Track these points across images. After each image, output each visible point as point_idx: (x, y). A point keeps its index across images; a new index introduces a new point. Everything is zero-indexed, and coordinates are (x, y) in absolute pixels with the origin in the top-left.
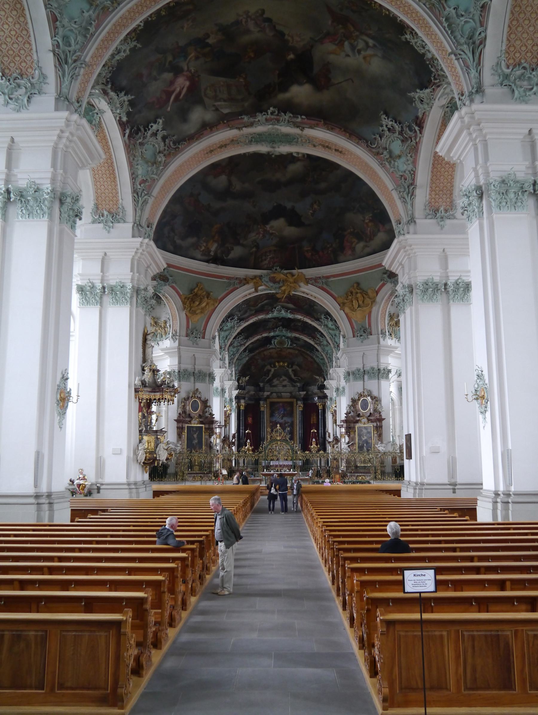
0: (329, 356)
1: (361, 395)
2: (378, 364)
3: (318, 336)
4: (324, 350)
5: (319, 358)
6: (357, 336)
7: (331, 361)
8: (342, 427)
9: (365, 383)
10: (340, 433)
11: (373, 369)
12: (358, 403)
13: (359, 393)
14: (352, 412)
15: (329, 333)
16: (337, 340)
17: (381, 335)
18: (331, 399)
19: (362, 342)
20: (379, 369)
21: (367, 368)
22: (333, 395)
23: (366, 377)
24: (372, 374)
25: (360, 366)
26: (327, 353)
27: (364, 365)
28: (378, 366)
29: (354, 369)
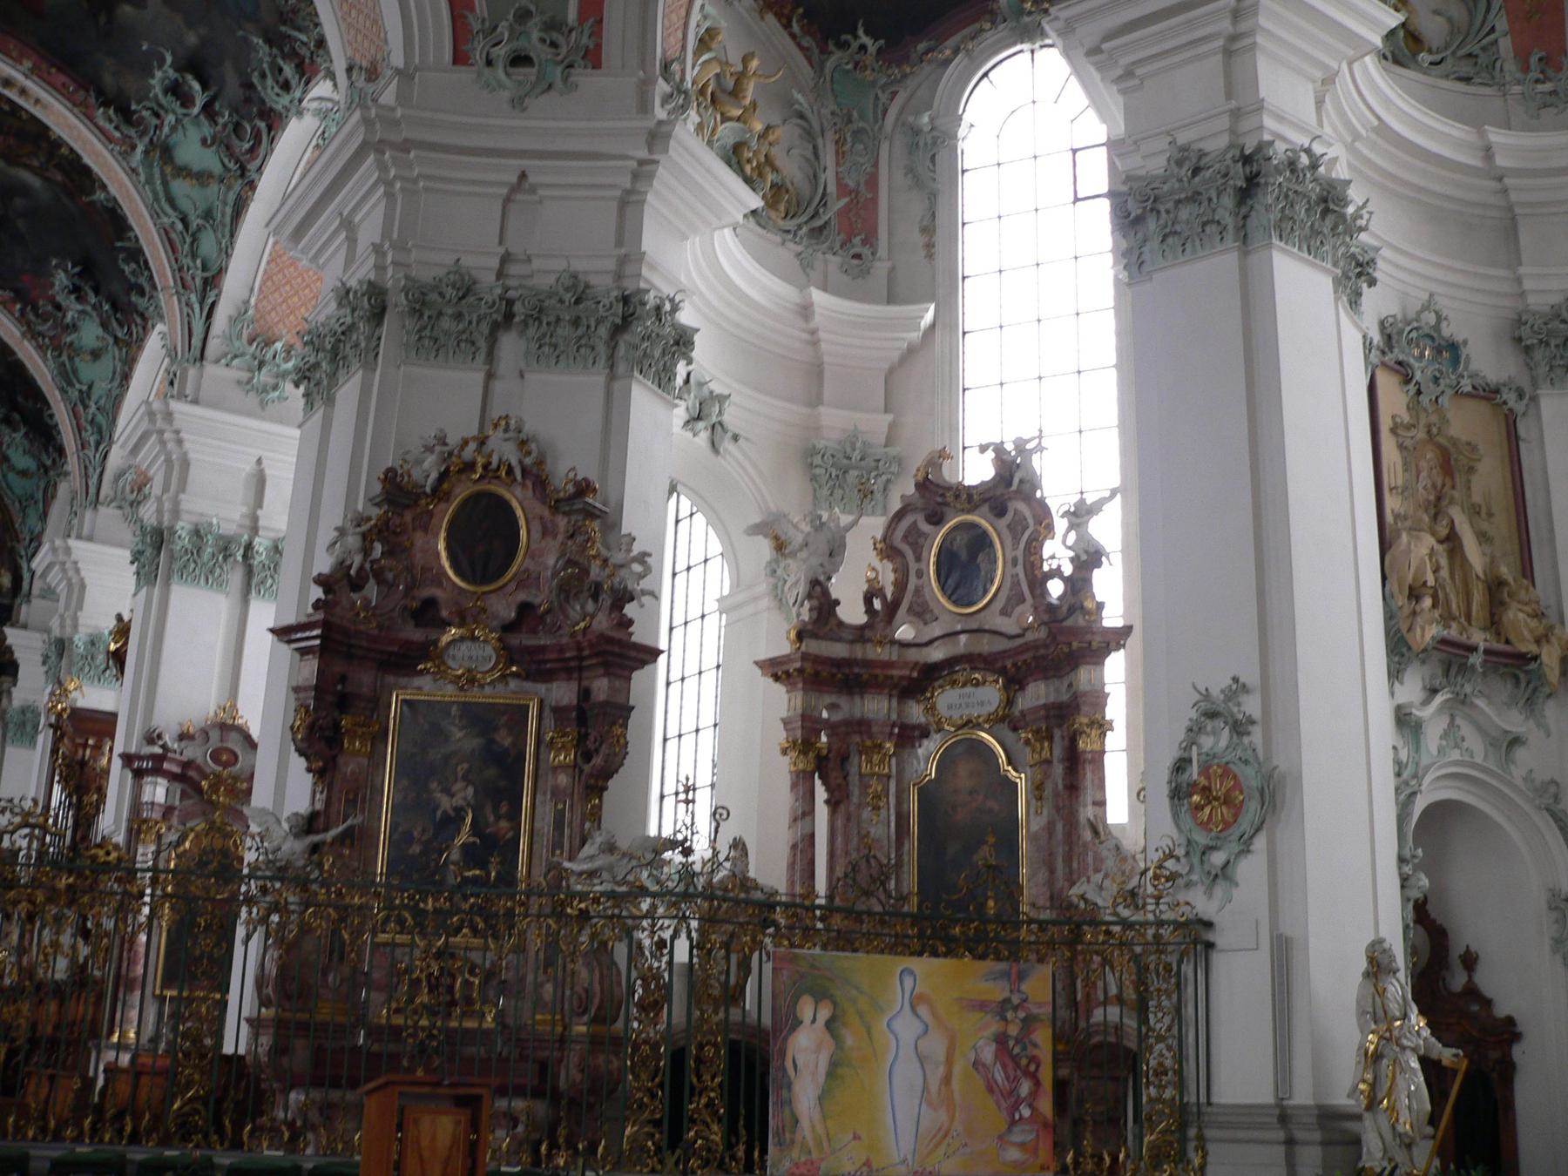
0: (93, 409)
1: (454, 469)
2: (623, 260)
3: (61, 279)
4: (67, 376)
5: (12, 468)
6: (489, 63)
7: (98, 444)
8: (157, 771)
9: (498, 386)
10: (136, 805)
11: (579, 292)
12: (425, 523)
13: (453, 440)
14: (372, 582)
15: (171, 201)
16: (208, 244)
17: (662, 87)
18: (62, 646)
19: (518, 103)
20: (626, 300)
21: (544, 273)
22: (75, 627)
23: (510, 346)
24: (564, 331)
25: (482, 266)
26: (84, 397)
27: (506, 259)
28: (619, 276)
29: (426, 275)
